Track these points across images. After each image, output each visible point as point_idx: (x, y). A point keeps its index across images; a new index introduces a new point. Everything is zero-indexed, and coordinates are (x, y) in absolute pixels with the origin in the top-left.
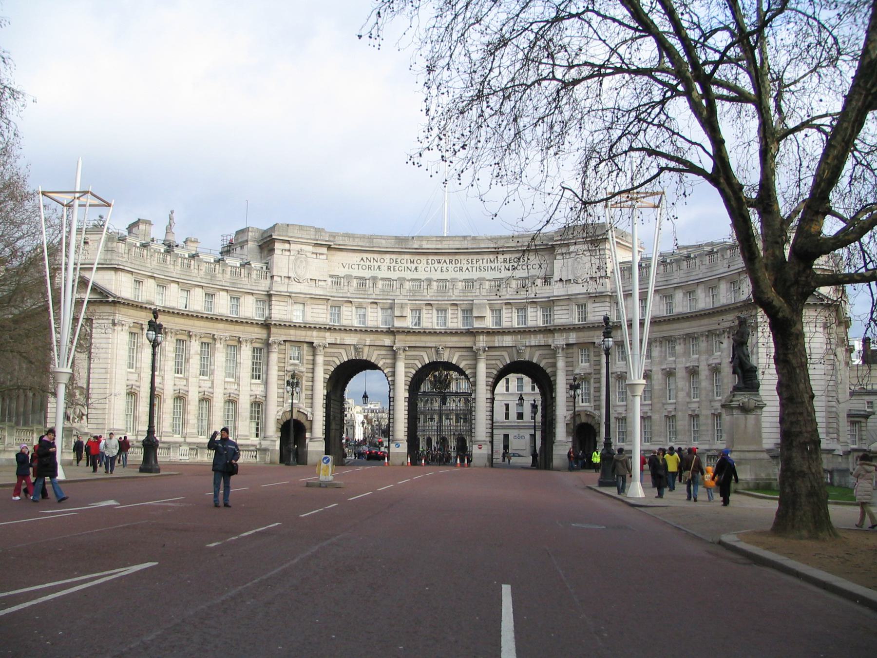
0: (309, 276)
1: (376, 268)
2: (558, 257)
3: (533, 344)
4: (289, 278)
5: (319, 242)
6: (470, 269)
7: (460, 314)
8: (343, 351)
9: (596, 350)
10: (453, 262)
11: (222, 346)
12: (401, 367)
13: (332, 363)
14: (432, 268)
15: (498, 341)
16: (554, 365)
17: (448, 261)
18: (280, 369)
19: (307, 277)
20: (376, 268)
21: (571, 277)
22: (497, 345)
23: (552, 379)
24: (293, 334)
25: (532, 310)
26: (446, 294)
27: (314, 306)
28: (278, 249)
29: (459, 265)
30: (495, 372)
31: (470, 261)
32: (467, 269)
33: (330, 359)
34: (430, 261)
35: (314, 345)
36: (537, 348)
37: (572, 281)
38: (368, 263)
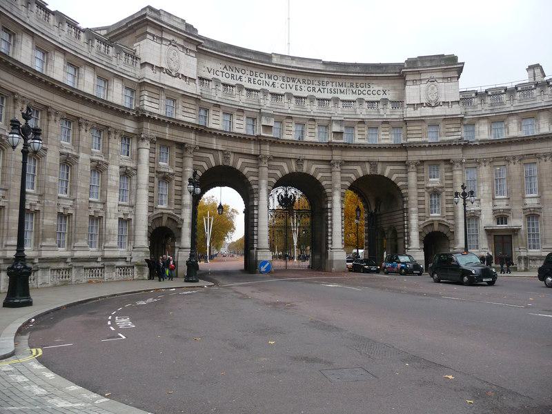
0: (181, 72)
2: (408, 83)
4: (161, 69)
5: (191, 37)
6: (322, 90)
7: (316, 130)
9: (448, 166)
14: (288, 86)
15: (351, 155)
16: (406, 179)
18: (152, 170)
19: (179, 72)
20: (238, 78)
21: (424, 101)
23: (403, 191)
24: (167, 133)
28: (150, 34)
31: (321, 83)
32: (319, 90)
33: (200, 163)
35: (186, 146)
37: (425, 105)
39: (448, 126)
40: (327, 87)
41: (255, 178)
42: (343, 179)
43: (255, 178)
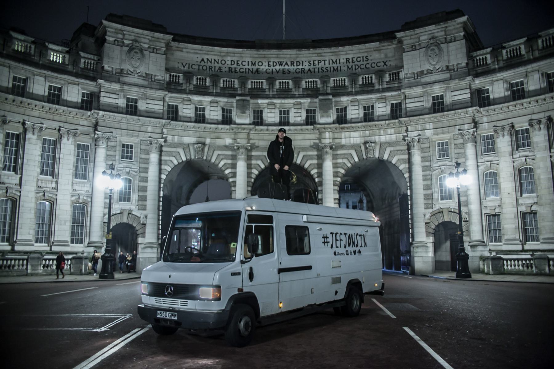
1: (216, 70)
3: (383, 139)
8: (181, 151)
10: (295, 64)
11: (35, 137)
12: (241, 166)
13: (169, 163)
17: (289, 63)
20: (216, 70)
22: (344, 142)
25: (380, 105)
26: (290, 93)
27: (149, 101)
29: (300, 67)
30: (343, 171)
31: (312, 63)
34: (271, 64)
36: (387, 145)
38: (209, 64)
39: (454, 93)
40: (317, 66)
41: (233, 171)
42: (335, 166)
43: (233, 171)
